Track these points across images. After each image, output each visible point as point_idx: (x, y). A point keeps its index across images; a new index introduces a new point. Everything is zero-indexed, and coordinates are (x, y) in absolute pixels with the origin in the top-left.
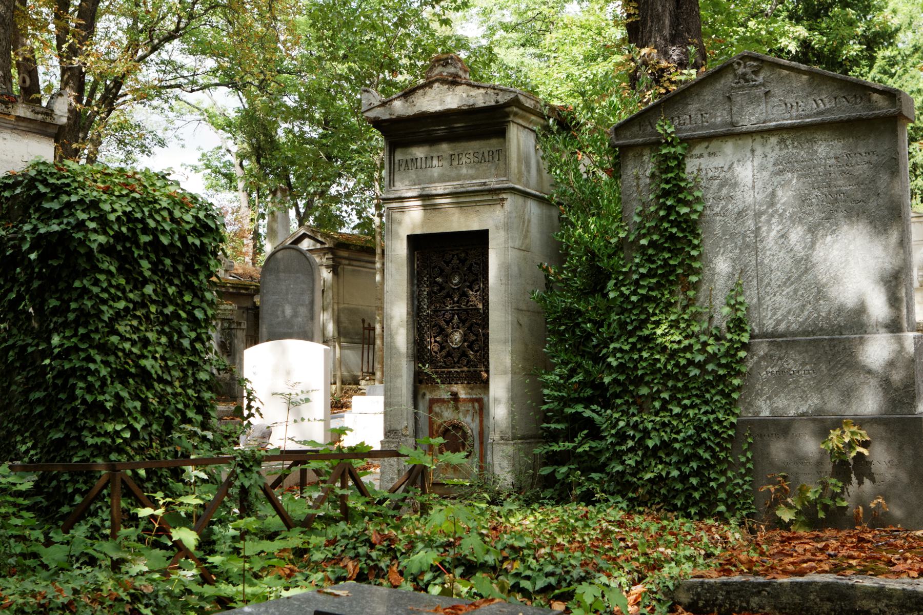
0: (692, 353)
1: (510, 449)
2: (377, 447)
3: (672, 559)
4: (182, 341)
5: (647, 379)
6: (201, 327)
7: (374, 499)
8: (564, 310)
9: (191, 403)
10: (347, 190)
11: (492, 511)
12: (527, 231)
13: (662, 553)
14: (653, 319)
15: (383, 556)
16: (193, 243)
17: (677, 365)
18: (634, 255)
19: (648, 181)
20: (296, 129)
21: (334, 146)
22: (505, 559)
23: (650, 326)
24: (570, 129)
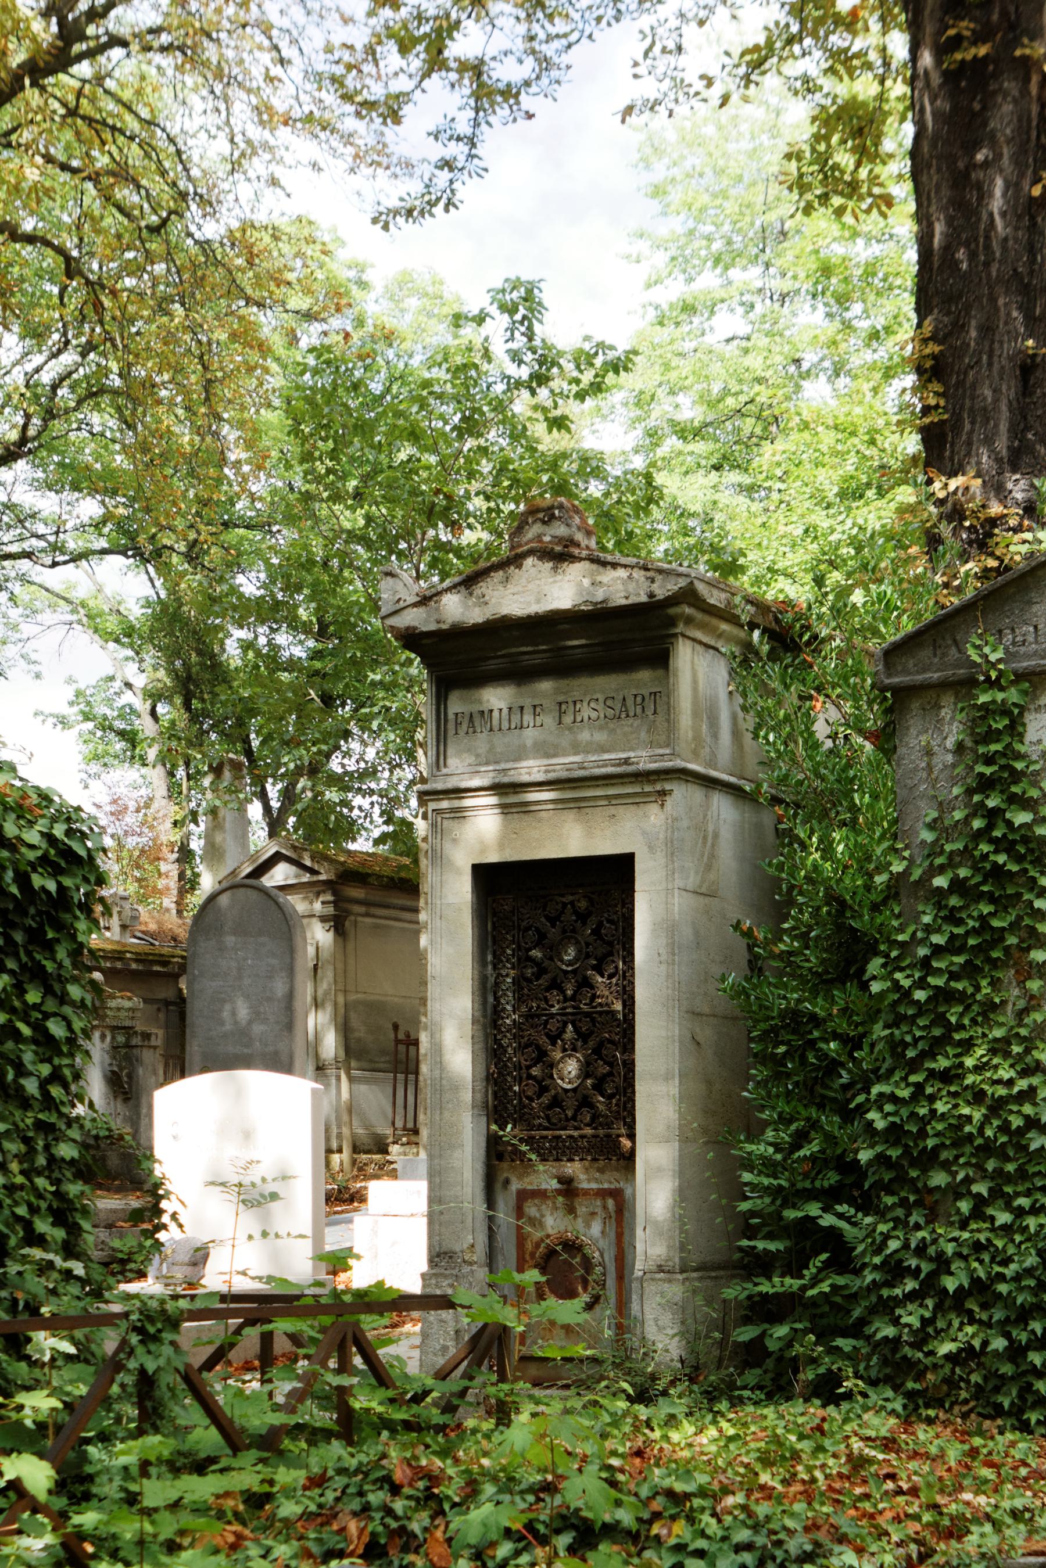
0: (1035, 1104)
1: (675, 1291)
2: (415, 1287)
3: (988, 1517)
4: (22, 1081)
5: (944, 1155)
6: (60, 1054)
7: (406, 1393)
8: (783, 1014)
9: (43, 1205)
10: (362, 765)
11: (636, 1417)
12: (712, 856)
13: (968, 1503)
14: (957, 1037)
15: (416, 1510)
16: (43, 888)
17: (1005, 1128)
18: (920, 908)
19: (950, 758)
20: (262, 641)
21: (337, 675)
22: (657, 1516)
23: (951, 1051)
24: (800, 650)
